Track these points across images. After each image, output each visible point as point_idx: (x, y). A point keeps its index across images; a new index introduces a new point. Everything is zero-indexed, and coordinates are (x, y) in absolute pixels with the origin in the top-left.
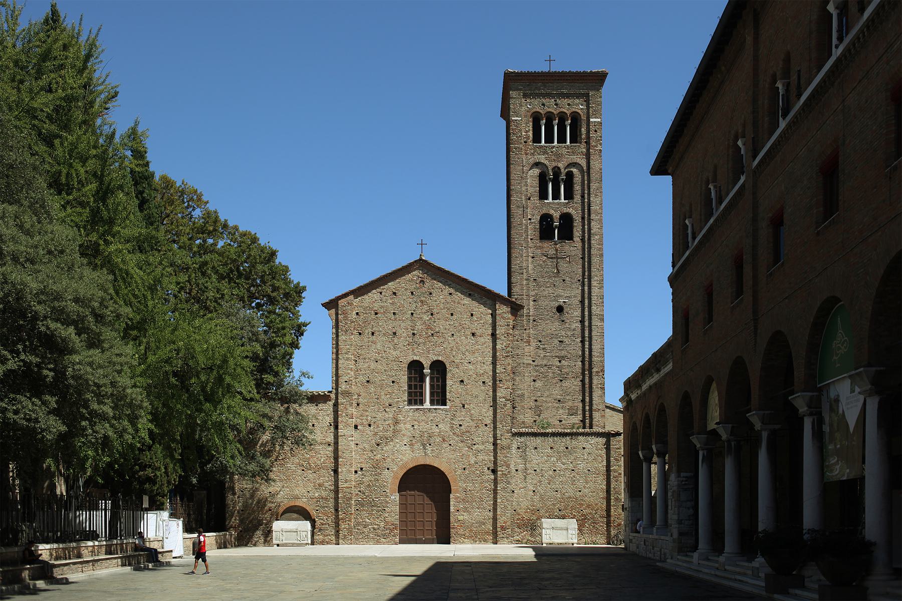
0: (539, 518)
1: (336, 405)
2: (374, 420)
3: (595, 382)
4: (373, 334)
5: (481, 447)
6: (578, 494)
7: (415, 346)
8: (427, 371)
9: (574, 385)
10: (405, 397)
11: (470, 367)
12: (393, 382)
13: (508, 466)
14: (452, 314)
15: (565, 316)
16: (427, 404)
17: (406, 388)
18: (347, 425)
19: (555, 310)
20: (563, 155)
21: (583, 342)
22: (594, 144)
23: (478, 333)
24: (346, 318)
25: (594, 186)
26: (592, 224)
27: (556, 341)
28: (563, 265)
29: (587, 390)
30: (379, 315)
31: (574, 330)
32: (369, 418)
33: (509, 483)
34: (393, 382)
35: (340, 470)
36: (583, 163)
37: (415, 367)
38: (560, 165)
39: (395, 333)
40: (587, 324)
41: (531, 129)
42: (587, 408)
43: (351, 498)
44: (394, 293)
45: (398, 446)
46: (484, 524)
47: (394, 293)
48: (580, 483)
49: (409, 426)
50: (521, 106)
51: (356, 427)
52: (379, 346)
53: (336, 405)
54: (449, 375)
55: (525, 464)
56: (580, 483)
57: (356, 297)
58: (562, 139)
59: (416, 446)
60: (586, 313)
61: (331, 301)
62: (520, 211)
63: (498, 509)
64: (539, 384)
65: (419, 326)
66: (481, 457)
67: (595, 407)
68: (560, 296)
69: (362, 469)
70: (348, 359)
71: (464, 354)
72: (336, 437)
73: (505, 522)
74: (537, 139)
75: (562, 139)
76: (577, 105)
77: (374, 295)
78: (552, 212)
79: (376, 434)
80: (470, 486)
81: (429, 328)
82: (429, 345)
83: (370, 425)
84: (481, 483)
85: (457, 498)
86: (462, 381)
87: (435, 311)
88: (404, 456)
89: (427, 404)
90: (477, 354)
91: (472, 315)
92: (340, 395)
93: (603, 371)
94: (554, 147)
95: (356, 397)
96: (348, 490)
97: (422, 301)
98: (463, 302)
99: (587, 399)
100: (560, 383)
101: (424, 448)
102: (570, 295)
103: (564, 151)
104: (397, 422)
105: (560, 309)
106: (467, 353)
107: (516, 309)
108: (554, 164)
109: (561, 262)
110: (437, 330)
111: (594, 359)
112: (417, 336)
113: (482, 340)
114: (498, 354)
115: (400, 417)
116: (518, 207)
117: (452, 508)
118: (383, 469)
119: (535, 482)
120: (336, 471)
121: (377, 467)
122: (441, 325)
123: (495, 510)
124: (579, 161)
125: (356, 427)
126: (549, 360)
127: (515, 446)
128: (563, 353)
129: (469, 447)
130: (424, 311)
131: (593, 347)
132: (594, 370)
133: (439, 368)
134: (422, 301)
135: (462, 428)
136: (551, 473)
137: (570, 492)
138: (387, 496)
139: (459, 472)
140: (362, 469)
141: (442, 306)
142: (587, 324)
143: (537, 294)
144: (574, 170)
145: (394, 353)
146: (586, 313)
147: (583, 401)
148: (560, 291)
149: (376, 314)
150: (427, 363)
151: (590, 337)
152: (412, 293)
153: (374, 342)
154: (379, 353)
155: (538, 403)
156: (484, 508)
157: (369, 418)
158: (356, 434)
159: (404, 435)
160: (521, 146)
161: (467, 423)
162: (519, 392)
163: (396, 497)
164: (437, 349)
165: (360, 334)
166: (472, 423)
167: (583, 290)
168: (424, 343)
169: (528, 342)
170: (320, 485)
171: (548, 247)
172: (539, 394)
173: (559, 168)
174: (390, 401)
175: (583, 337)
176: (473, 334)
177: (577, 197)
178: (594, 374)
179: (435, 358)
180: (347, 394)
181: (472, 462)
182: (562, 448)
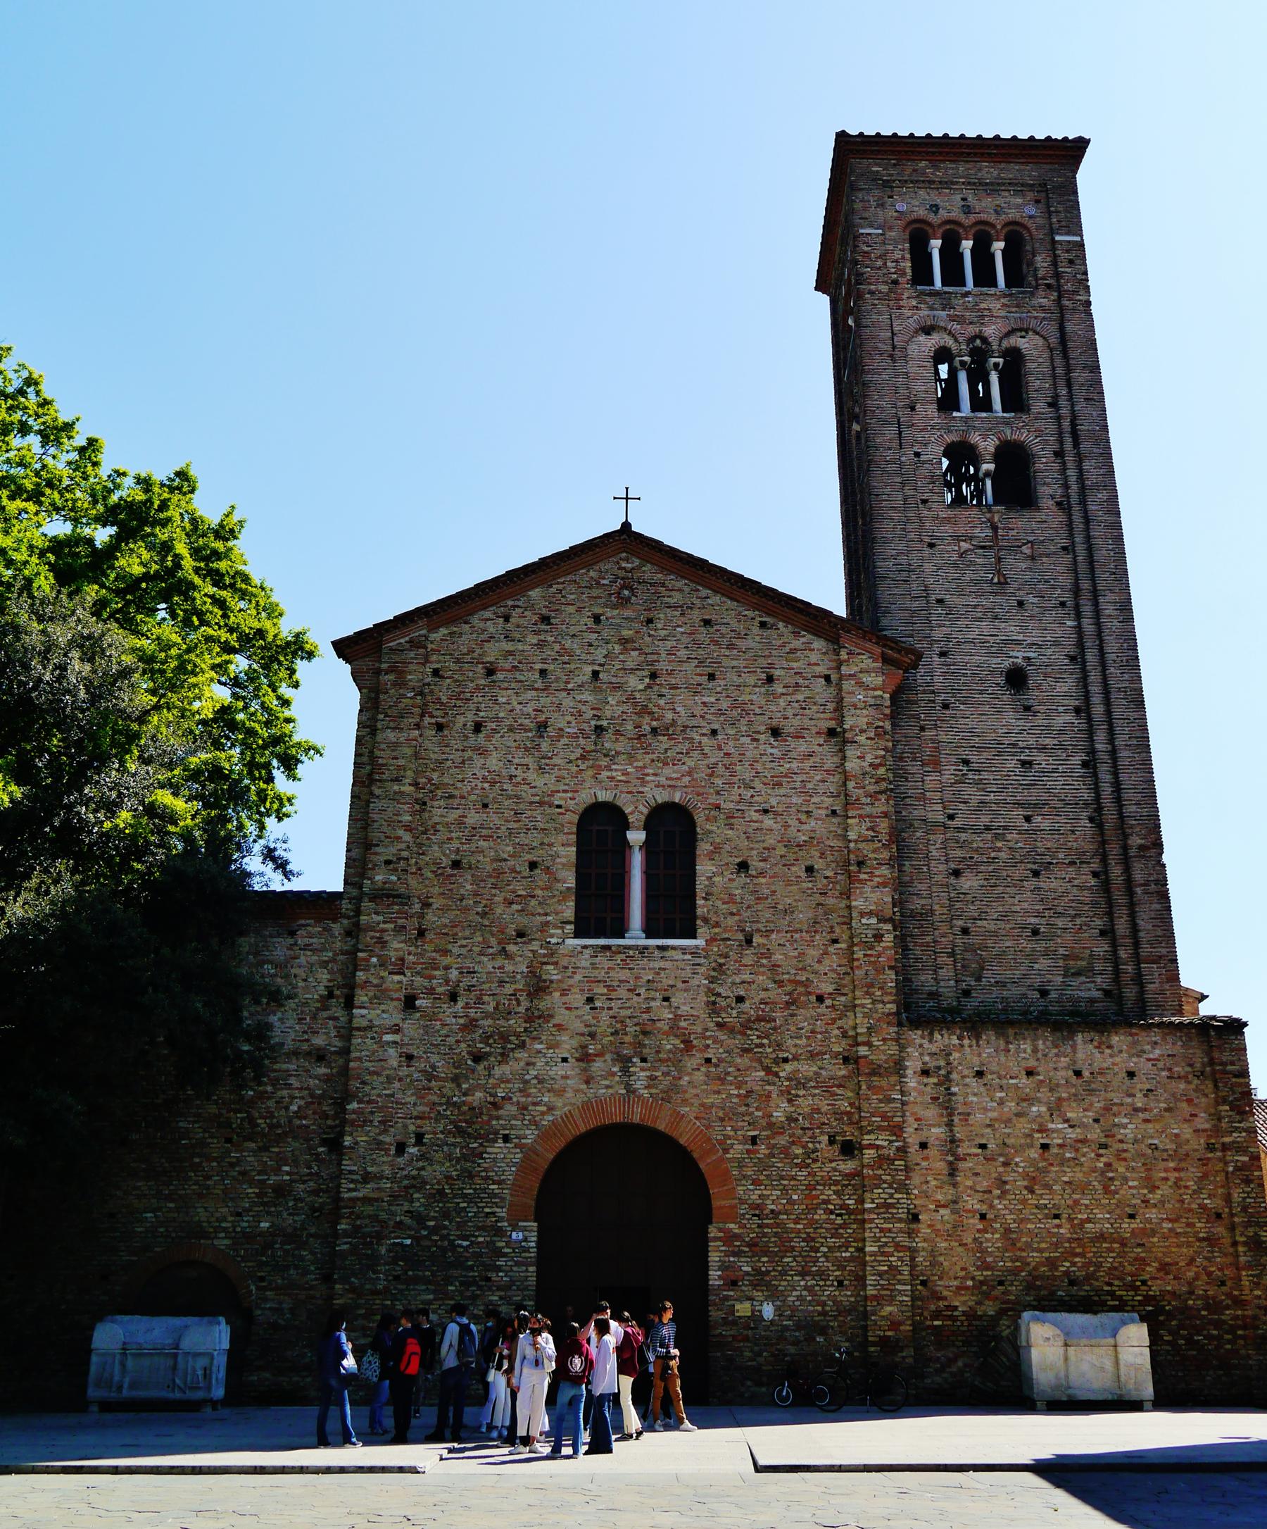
0: (1013, 1311)
1: (353, 932)
2: (467, 981)
3: (1138, 876)
4: (478, 727)
5: (807, 1069)
6: (1127, 1225)
7: (604, 762)
8: (636, 837)
9: (1071, 884)
10: (569, 911)
11: (768, 822)
12: (533, 865)
13: (897, 1130)
14: (712, 677)
15: (1033, 697)
16: (635, 936)
17: (571, 883)
18: (381, 995)
19: (1001, 680)
20: (994, 315)
21: (1090, 765)
22: (1068, 287)
23: (790, 726)
24: (400, 683)
25: (1079, 376)
26: (1086, 465)
27: (1012, 764)
28: (1016, 566)
29: (1119, 898)
30: (500, 676)
31: (1061, 732)
32: (454, 974)
33: (903, 1187)
34: (533, 865)
35: (348, 1141)
36: (1052, 329)
37: (600, 827)
38: (990, 331)
39: (542, 726)
40: (1098, 709)
41: (908, 256)
42: (1123, 954)
43: (379, 1237)
44: (545, 619)
45: (540, 1063)
46: (823, 1331)
47: (545, 619)
48: (1131, 1191)
49: (577, 999)
50: (882, 206)
51: (409, 1003)
52: (493, 762)
53: (353, 932)
54: (703, 847)
55: (950, 1125)
56: (1131, 1191)
57: (433, 628)
58: (985, 276)
59: (598, 1066)
60: (1095, 689)
61: (361, 636)
62: (890, 432)
63: (871, 1280)
64: (969, 882)
65: (614, 705)
66: (805, 1104)
67: (1145, 950)
68: (1018, 642)
69: (419, 1138)
70: (397, 797)
71: (749, 787)
72: (347, 1033)
73: (895, 1325)
74: (922, 274)
75: (985, 276)
76: (1018, 207)
77: (487, 621)
78: (975, 438)
79: (471, 1025)
80: (773, 1200)
81: (645, 711)
82: (643, 759)
83: (453, 997)
84: (810, 1187)
85: (729, 1238)
86: (743, 866)
87: (658, 666)
88: (557, 1088)
89: (635, 936)
90: (782, 791)
91: (770, 679)
92: (366, 904)
93: (1158, 846)
94: (967, 294)
95: (417, 907)
96: (369, 1209)
97: (624, 642)
98: (742, 644)
99: (1122, 926)
100: (1031, 884)
101: (625, 1071)
102: (1040, 638)
103: (995, 305)
104: (538, 988)
105: (1016, 679)
106: (758, 784)
107: (901, 658)
108: (972, 330)
109: (1009, 561)
110: (669, 716)
111: (1130, 809)
112: (608, 735)
113: (803, 747)
114: (851, 785)
115: (552, 973)
116: (886, 422)
117: (715, 1276)
118: (489, 1137)
119: (985, 1184)
120: (335, 1145)
121: (473, 1128)
122: (681, 707)
123: (861, 1280)
124: (1033, 323)
125: (409, 1003)
126: (996, 814)
127: (913, 1065)
128: (1034, 795)
129: (768, 1070)
130: (630, 665)
131: (1123, 777)
132: (1135, 841)
133: (674, 829)
134: (624, 642)
135: (746, 1005)
136: (1034, 1153)
137: (1102, 1221)
138: (500, 1232)
139: (738, 1150)
140: (419, 1138)
141: (683, 653)
142: (1098, 709)
143: (948, 638)
144: (1022, 343)
145: (540, 782)
146: (1095, 689)
147: (1107, 933)
148: (1011, 629)
149: (490, 672)
150: (636, 812)
151: (1113, 753)
152: (597, 619)
153: (483, 752)
154: (493, 783)
155: (974, 940)
156: (822, 1274)
157: (454, 974)
158: (411, 1028)
159: (559, 1027)
160: (884, 288)
161: (761, 989)
162: (917, 904)
163: (526, 1235)
164: (668, 771)
165: (440, 727)
166: (775, 994)
167: (1079, 629)
168: (631, 757)
169: (936, 763)
170: (282, 1191)
171: (973, 523)
172: (973, 910)
173: (985, 340)
174: (524, 921)
175: (1092, 752)
176: (775, 732)
177: (1039, 405)
178: (1132, 852)
179: (662, 797)
180: (385, 896)
181: (779, 1115)
182: (1063, 1075)
